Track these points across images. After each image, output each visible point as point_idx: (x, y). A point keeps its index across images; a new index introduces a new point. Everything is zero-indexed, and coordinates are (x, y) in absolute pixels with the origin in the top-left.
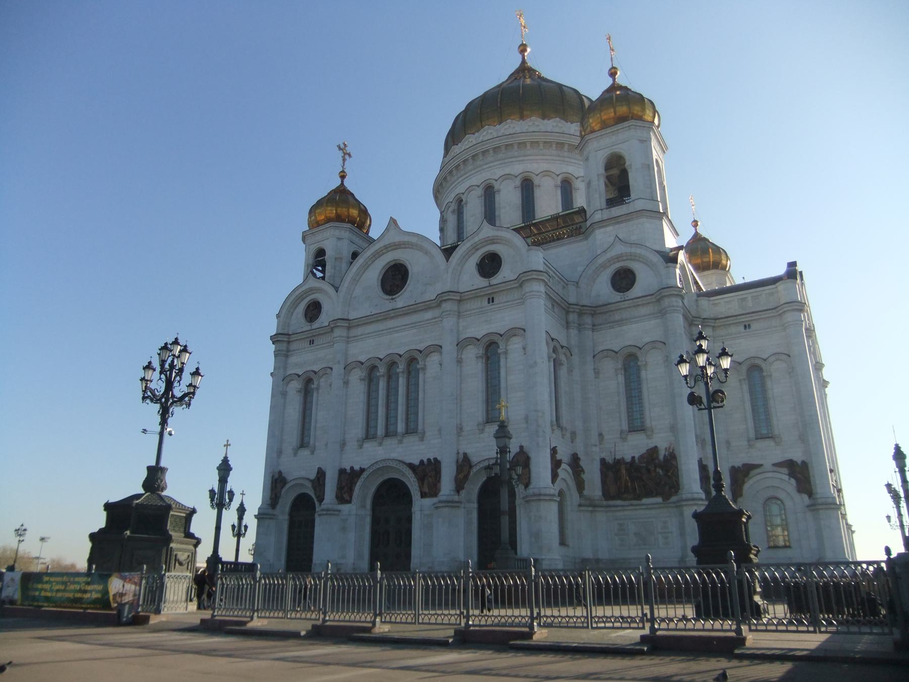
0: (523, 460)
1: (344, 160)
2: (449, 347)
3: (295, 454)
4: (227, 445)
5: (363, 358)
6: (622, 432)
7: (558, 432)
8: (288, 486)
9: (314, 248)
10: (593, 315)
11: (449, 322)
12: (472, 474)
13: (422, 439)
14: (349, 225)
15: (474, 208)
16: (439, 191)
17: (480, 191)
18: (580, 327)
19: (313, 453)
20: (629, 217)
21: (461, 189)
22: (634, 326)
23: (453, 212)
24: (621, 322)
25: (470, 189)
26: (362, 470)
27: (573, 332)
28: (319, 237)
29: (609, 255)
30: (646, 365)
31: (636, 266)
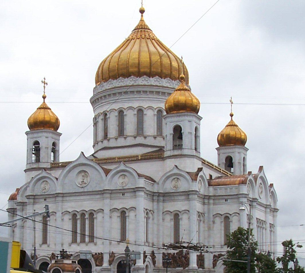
1: (44, 87)
2: (107, 210)
5: (70, 210)
8: (38, 259)
10: (163, 196)
11: (107, 201)
12: (115, 259)
13: (96, 244)
17: (116, 114)
18: (158, 201)
22: (179, 203)
23: (102, 119)
24: (174, 201)
25: (112, 110)
26: (72, 255)
27: (155, 203)
29: (171, 173)
30: (181, 219)
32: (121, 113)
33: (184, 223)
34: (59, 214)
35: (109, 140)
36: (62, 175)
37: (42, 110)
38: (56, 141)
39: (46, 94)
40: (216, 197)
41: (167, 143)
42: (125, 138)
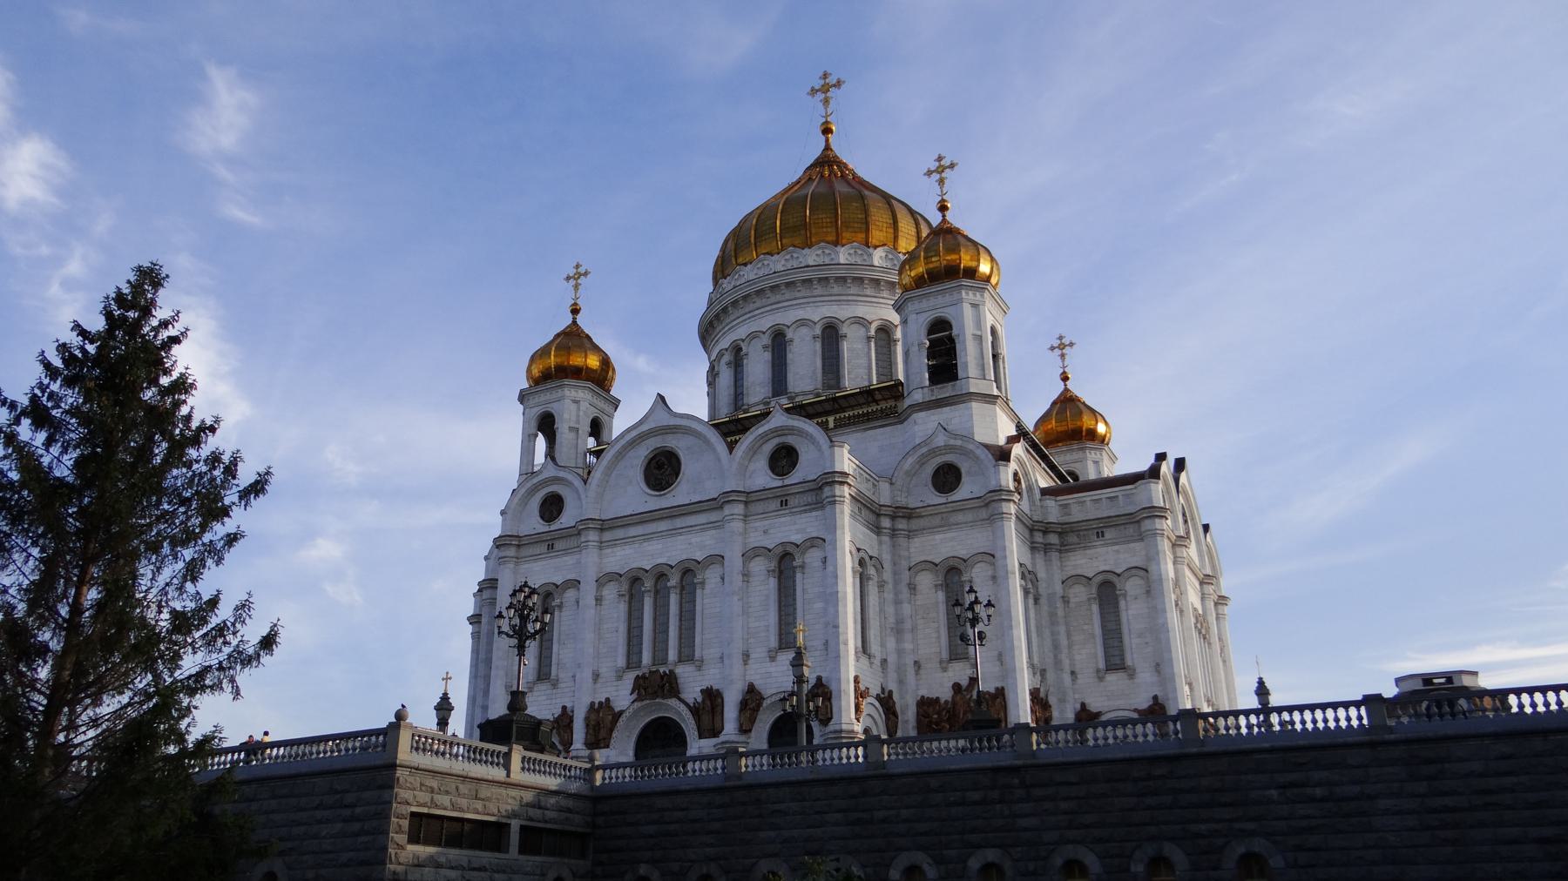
0: (823, 692)
4: (447, 679)
6: (941, 662)
7: (864, 660)
9: (536, 412)
13: (699, 668)
14: (589, 384)
15: (758, 367)
16: (708, 331)
17: (766, 340)
18: (894, 533)
19: (555, 685)
21: (741, 332)
23: (728, 364)
25: (753, 336)
27: (886, 539)
28: (543, 398)
38: (604, 418)
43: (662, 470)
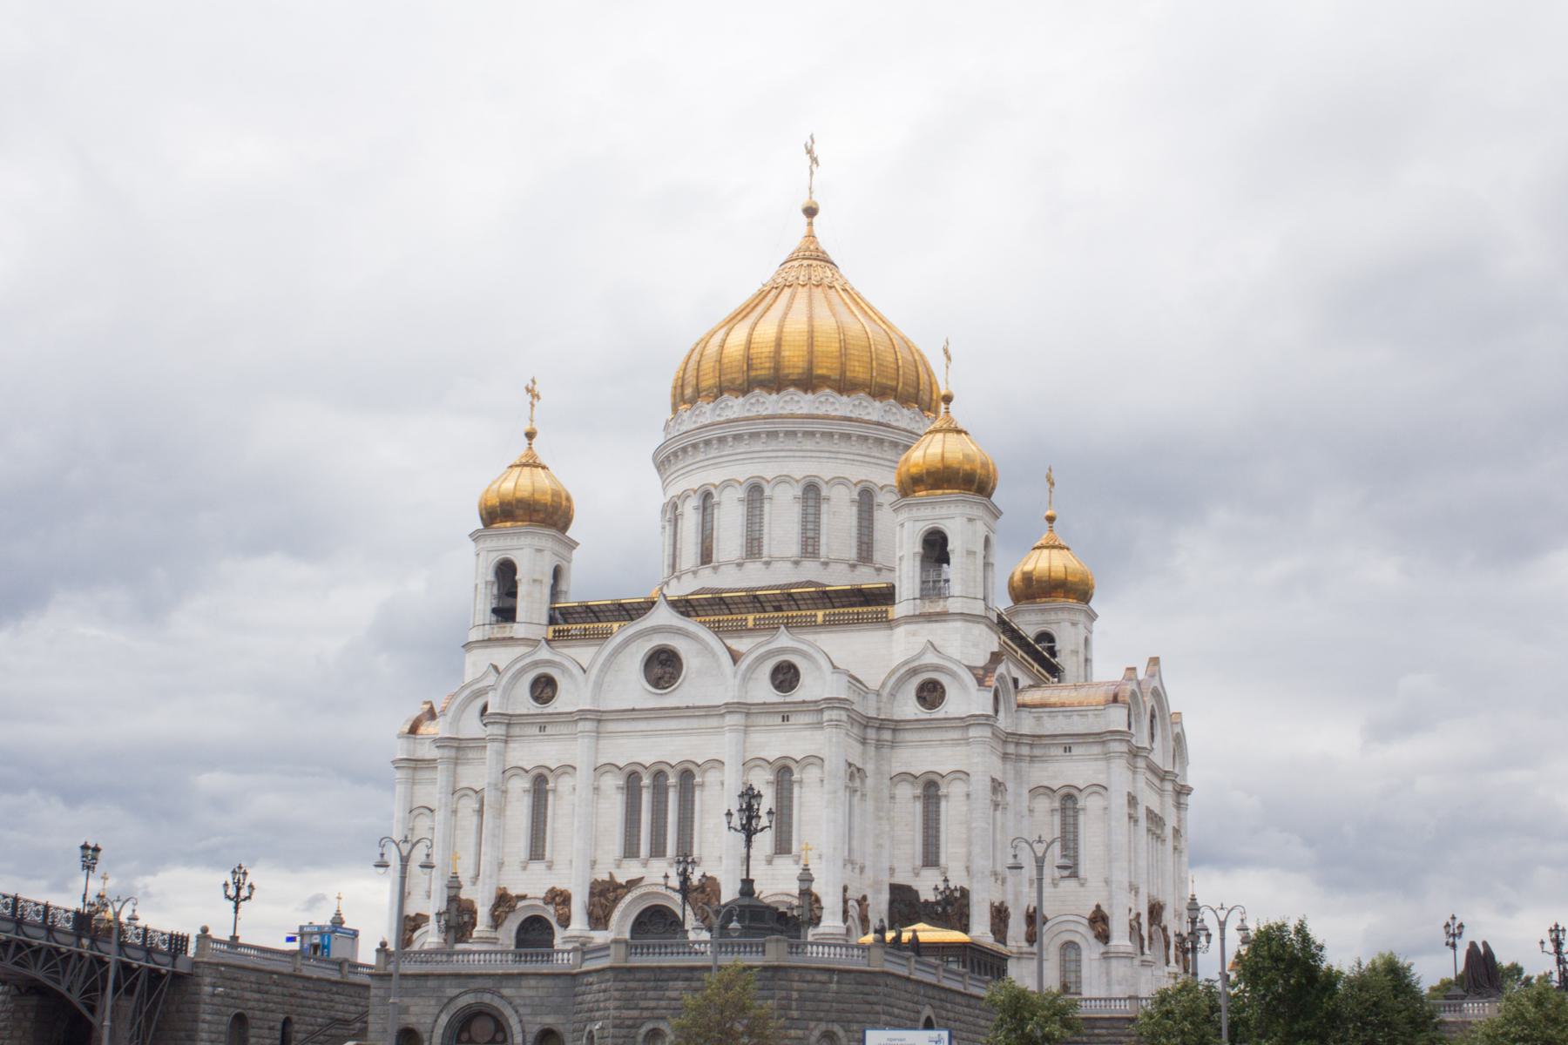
3: (524, 868)
9: (495, 558)
10: (894, 730)
16: (665, 461)
17: (741, 493)
18: (879, 745)
19: (550, 867)
20: (942, 616)
21: (713, 476)
23: (696, 508)
25: (727, 484)
27: (871, 751)
31: (944, 679)
32: (755, 493)
33: (952, 811)
34: (583, 776)
35: (715, 569)
36: (601, 660)
37: (527, 470)
38: (564, 564)
39: (536, 426)
40: (1036, 739)
41: (907, 577)
42: (767, 563)
43: (663, 666)
